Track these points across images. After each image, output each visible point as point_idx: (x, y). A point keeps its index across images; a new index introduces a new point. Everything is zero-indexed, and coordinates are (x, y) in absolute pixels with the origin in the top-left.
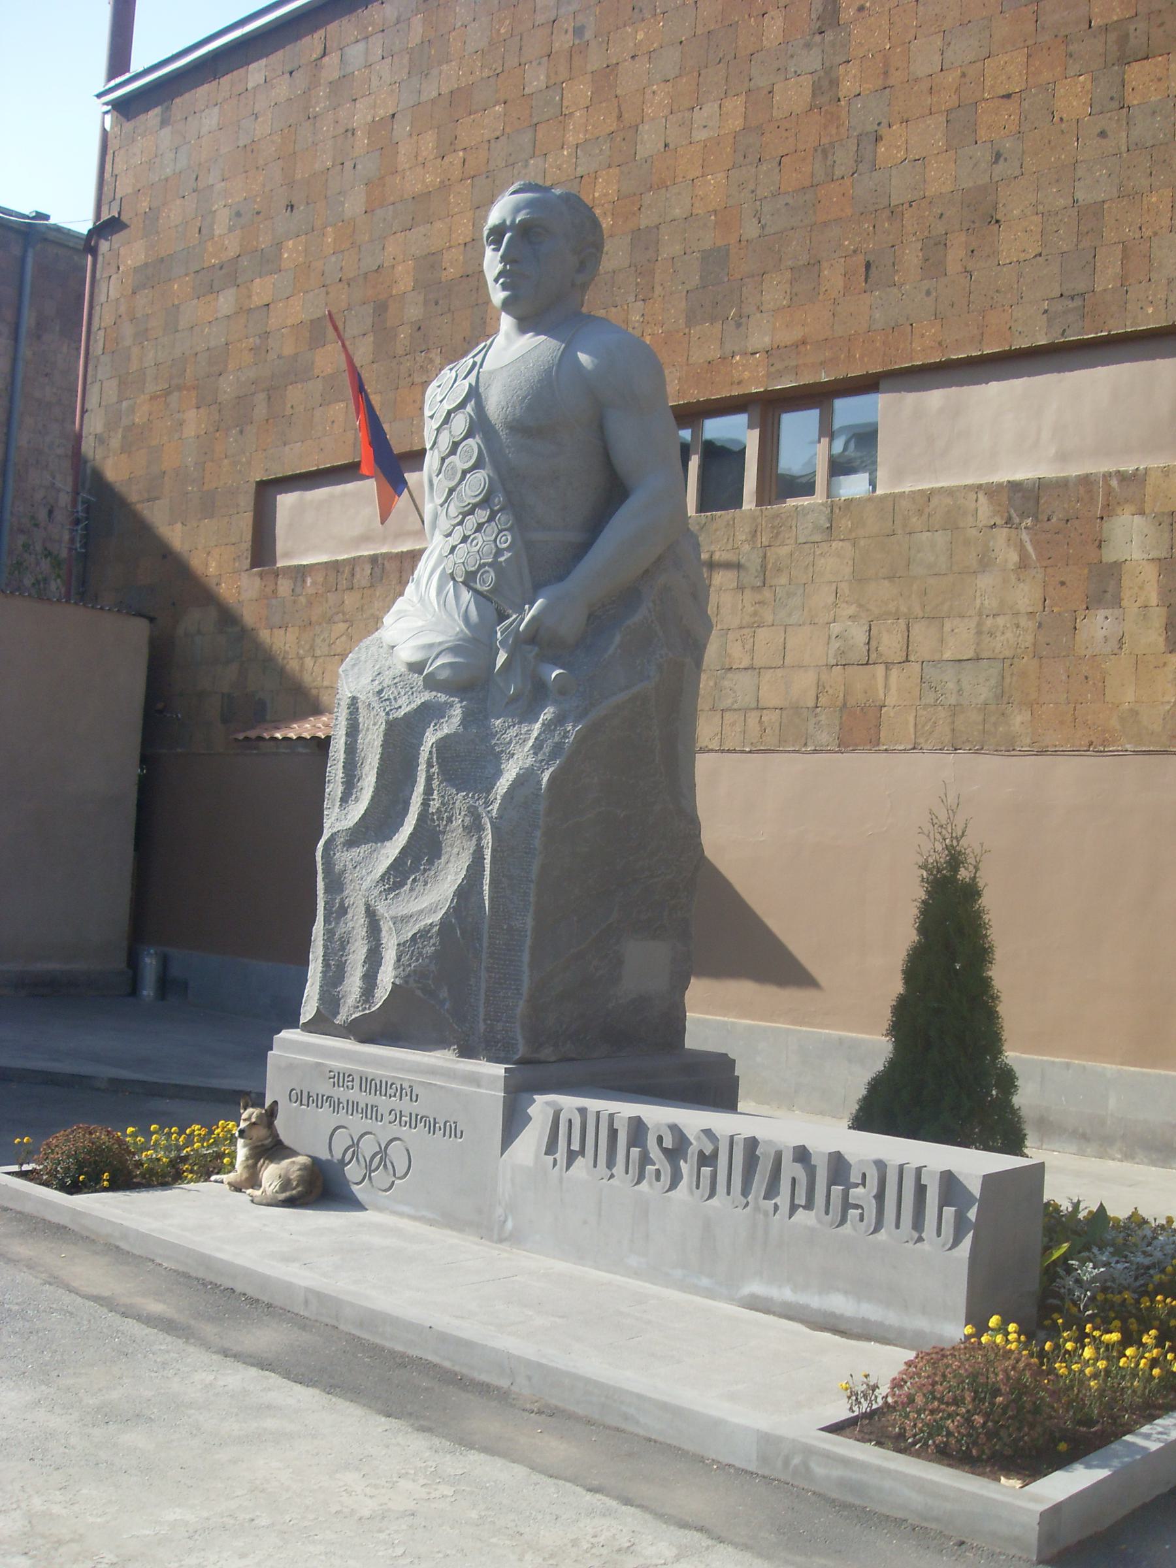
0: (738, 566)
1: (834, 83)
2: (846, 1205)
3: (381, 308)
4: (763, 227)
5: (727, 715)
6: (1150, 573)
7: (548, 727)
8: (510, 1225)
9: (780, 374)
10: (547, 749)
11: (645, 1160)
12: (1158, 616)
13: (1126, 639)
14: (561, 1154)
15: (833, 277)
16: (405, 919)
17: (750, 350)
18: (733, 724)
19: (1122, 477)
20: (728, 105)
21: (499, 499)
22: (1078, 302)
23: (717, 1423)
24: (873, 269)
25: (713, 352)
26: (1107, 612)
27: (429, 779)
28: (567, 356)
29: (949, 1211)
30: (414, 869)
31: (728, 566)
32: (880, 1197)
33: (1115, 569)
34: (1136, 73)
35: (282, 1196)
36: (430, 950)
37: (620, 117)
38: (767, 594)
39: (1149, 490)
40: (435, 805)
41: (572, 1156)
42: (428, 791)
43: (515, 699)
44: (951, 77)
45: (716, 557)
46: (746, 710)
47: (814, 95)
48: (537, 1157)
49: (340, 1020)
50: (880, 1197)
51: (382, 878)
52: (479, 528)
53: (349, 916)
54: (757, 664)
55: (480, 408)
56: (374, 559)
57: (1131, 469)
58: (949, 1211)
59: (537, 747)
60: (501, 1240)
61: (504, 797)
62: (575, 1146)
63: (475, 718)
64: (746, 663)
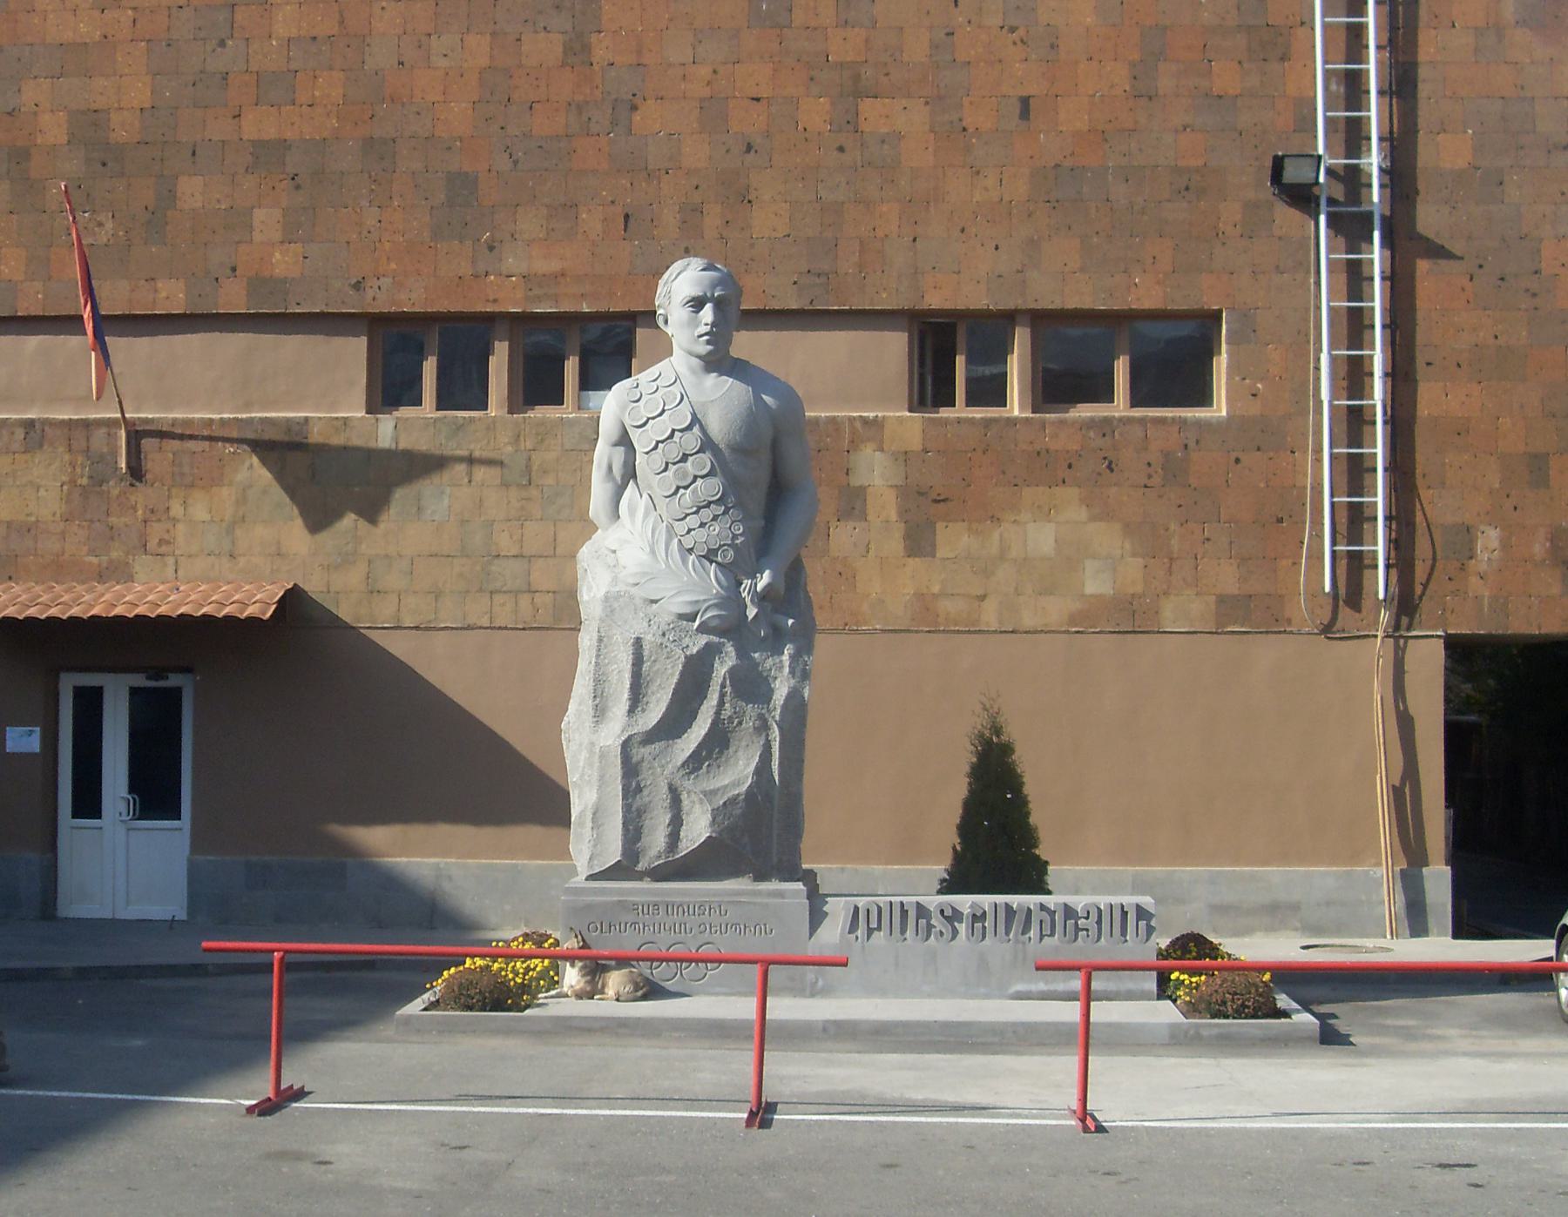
0: (501, 464)
1: (587, 48)
2: (1077, 929)
3: (20, 155)
4: (516, 163)
5: (497, 597)
6: (890, 497)
7: (793, 658)
8: (820, 983)
9: (539, 299)
10: (798, 674)
11: (930, 927)
12: (898, 531)
13: (872, 546)
14: (861, 931)
15: (591, 220)
16: (714, 792)
17: (505, 272)
18: (503, 605)
19: (865, 421)
20: (472, 40)
21: (731, 500)
22: (823, 279)
23: (1144, 1025)
24: (632, 220)
25: (466, 269)
26: (857, 524)
27: (722, 695)
28: (758, 398)
29: (1142, 924)
30: (709, 757)
31: (490, 462)
32: (1099, 922)
33: (861, 492)
34: (866, 106)
35: (640, 993)
36: (738, 812)
37: (342, 22)
38: (534, 492)
39: (887, 433)
40: (726, 714)
41: (870, 931)
42: (721, 703)
43: (764, 639)
44: (704, 71)
45: (477, 454)
46: (516, 593)
47: (565, 53)
48: (842, 935)
49: (640, 867)
50: (1099, 922)
51: (683, 766)
52: (715, 518)
53: (645, 792)
54: (526, 552)
55: (703, 430)
56: (29, 424)
57: (872, 415)
58: (1142, 924)
59: (792, 672)
60: (812, 995)
61: (784, 707)
62: (874, 925)
63: (742, 653)
64: (514, 552)
